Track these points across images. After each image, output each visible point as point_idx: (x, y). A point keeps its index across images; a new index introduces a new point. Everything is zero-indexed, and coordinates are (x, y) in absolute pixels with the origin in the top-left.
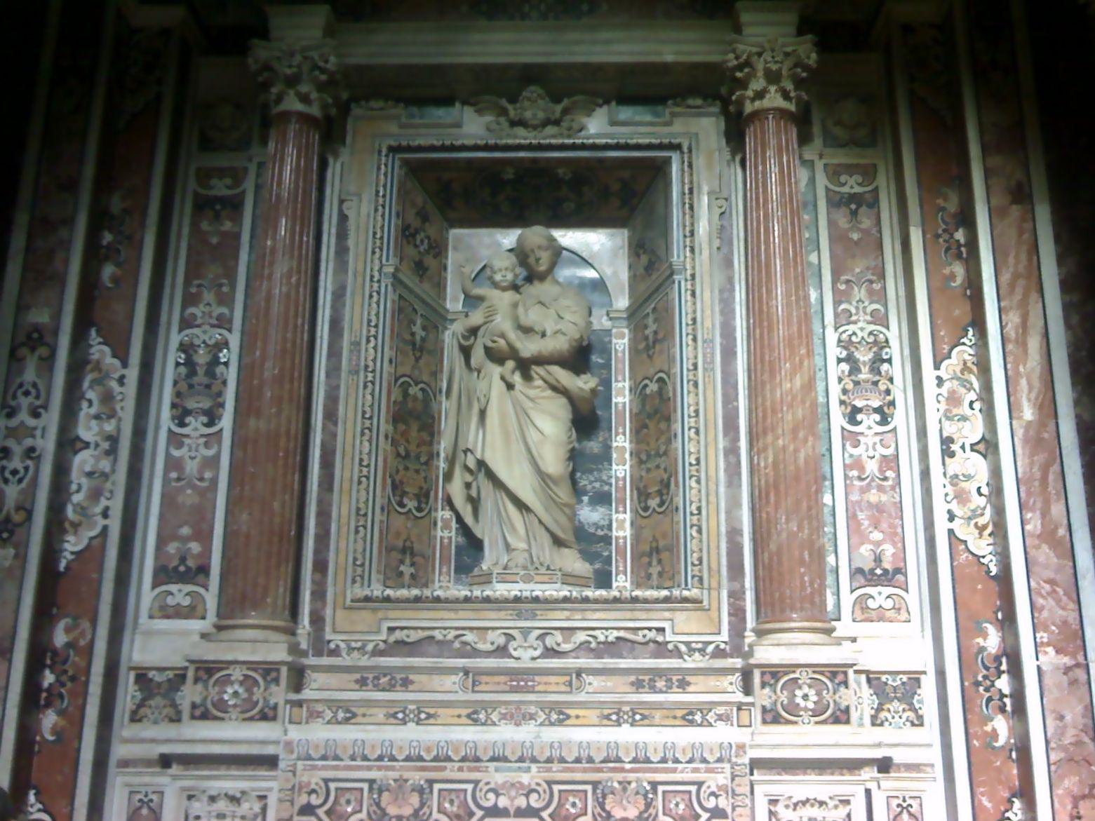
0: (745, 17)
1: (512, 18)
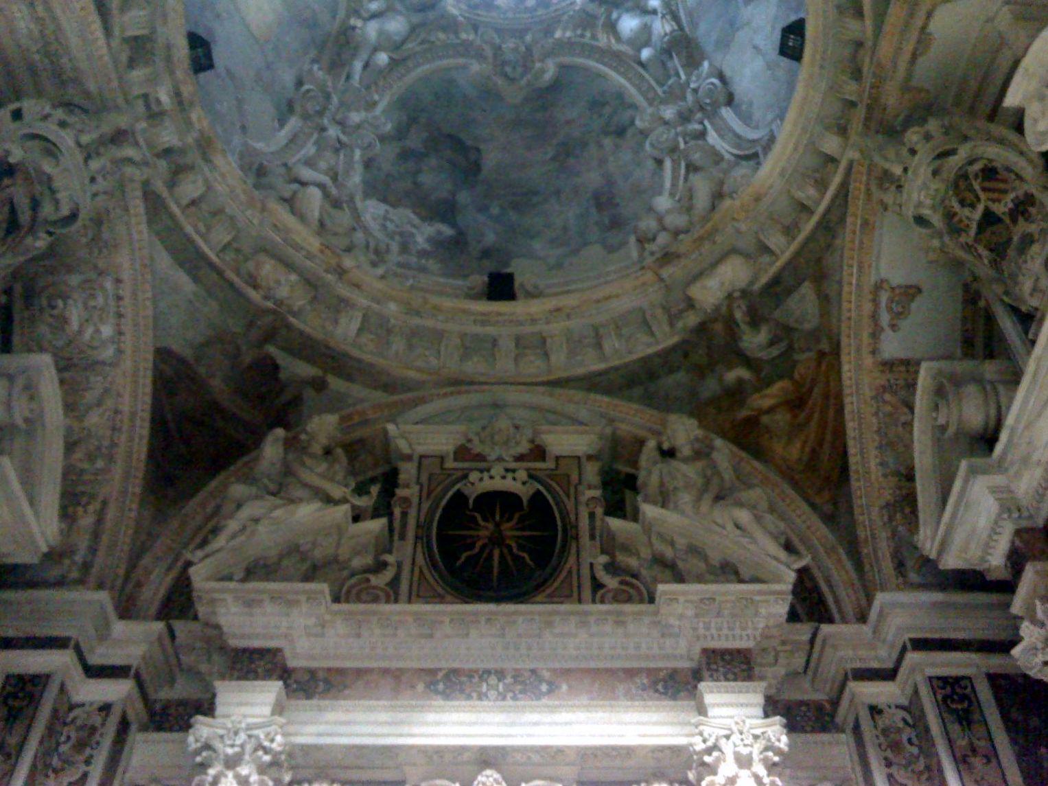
0: (709, 699)
1: (469, 697)
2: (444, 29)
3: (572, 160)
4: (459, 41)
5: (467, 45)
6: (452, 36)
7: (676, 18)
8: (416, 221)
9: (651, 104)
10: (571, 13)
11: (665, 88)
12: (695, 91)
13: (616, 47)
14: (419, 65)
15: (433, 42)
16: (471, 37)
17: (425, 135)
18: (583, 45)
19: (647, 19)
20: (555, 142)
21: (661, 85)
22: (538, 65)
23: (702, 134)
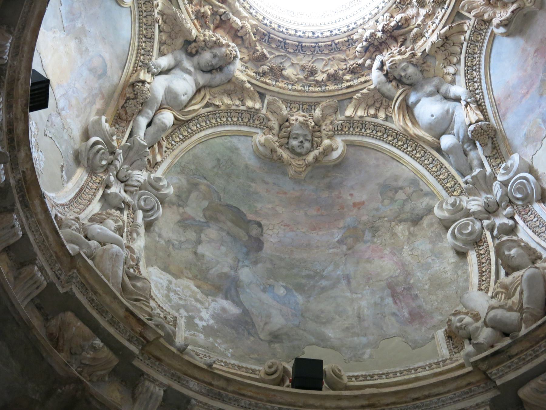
2: (229, 94)
3: (361, 247)
4: (242, 108)
5: (253, 113)
6: (238, 102)
7: (480, 106)
8: (199, 295)
9: (451, 194)
10: (365, 91)
11: (468, 178)
12: (505, 184)
13: (413, 130)
14: (202, 129)
15: (218, 106)
16: (258, 106)
17: (206, 203)
18: (375, 125)
19: (450, 105)
20: (341, 225)
21: (463, 175)
22: (327, 142)
23: (513, 230)
